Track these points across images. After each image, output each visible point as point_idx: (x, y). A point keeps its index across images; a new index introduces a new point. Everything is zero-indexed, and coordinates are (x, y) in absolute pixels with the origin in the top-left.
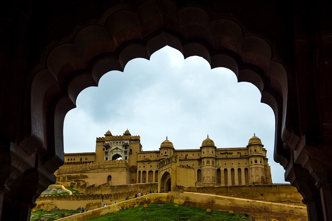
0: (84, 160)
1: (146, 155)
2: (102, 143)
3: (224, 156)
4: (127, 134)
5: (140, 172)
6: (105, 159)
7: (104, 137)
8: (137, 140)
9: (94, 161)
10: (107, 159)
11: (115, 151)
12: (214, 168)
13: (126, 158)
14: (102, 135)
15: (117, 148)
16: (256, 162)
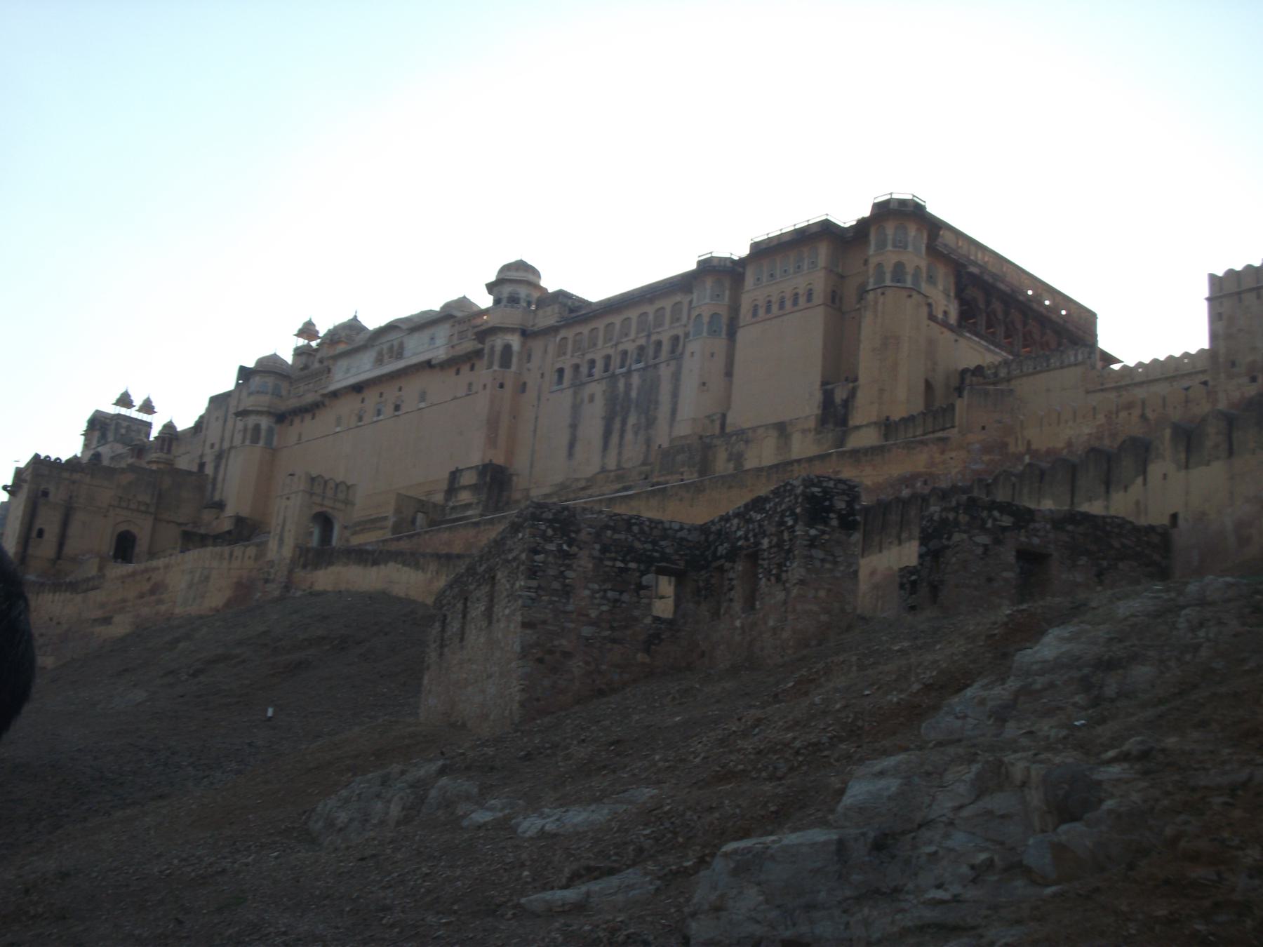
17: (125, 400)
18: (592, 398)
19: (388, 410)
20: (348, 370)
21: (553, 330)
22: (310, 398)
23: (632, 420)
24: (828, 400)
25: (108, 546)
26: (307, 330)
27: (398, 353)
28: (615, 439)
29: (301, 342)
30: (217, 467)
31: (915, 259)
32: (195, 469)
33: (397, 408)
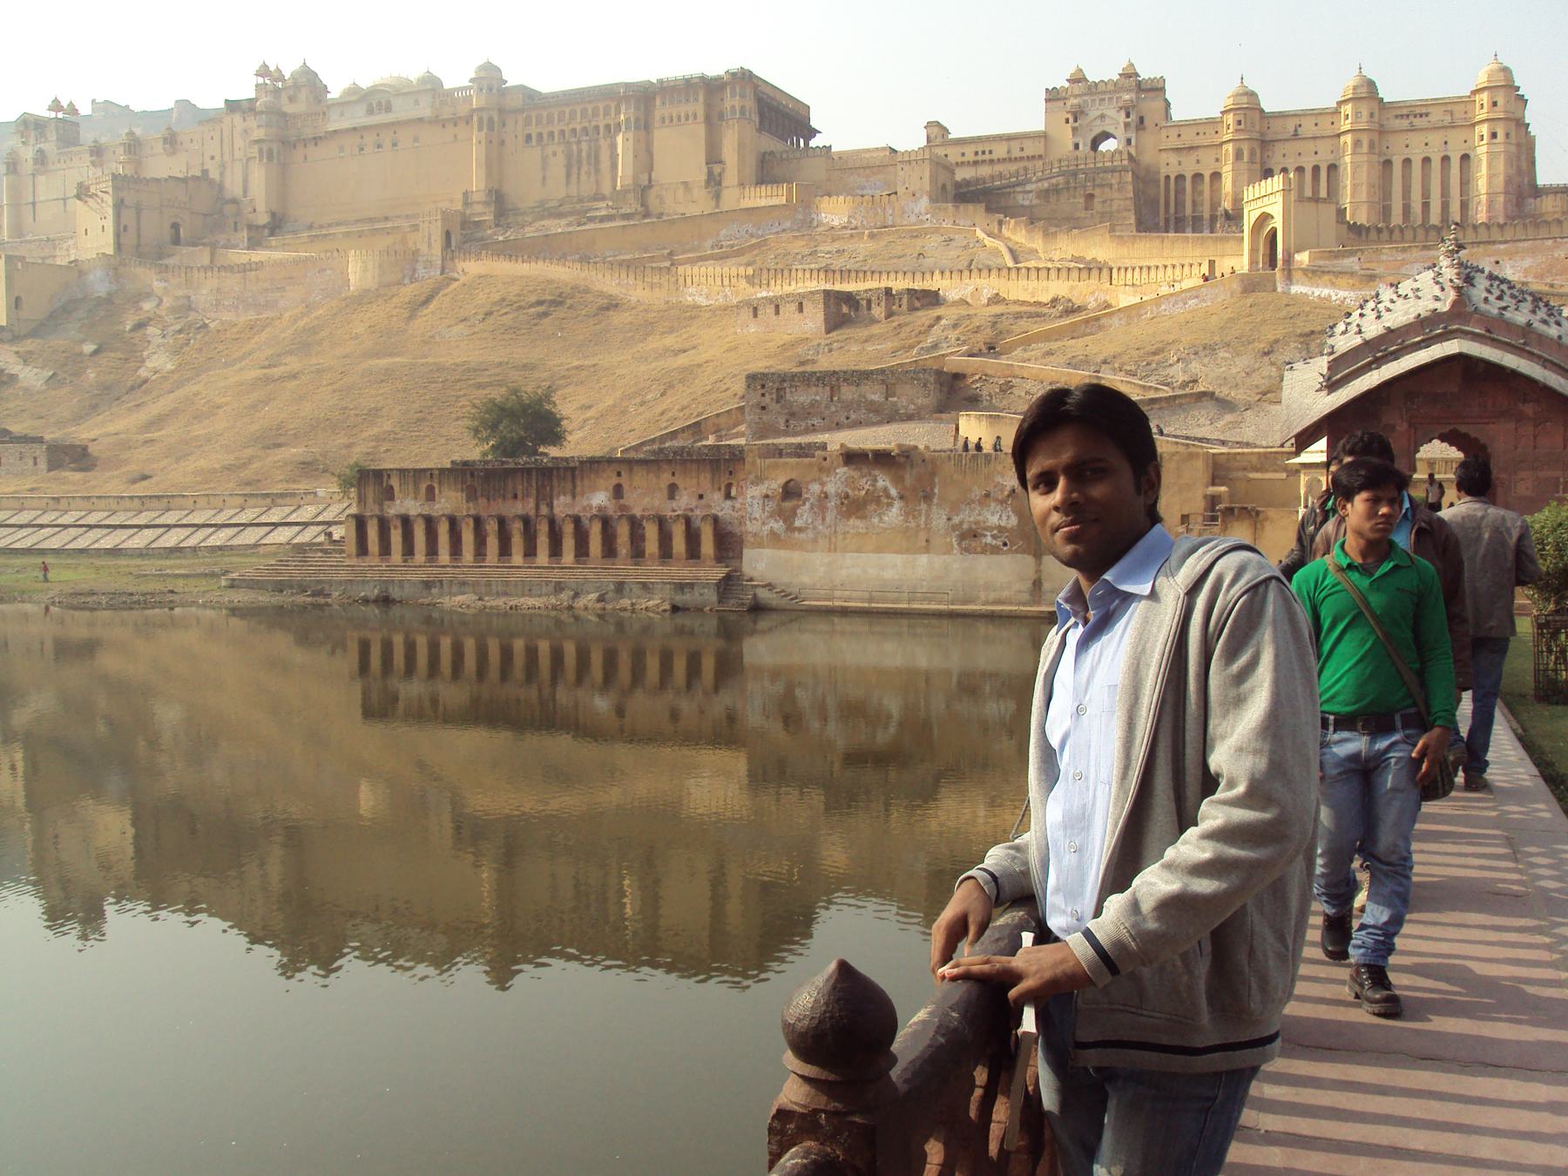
0: (1016, 153)
1: (1183, 131)
2: (1061, 103)
3: (1405, 123)
4: (1130, 74)
5: (1167, 177)
6: (1071, 147)
7: (1067, 85)
8: (1156, 89)
9: (1042, 152)
10: (1077, 146)
11: (1098, 122)
12: (1375, 158)
13: (1129, 142)
14: (1061, 82)
15: (1102, 117)
16: (1494, 135)
17: (56, 106)
18: (555, 154)
19: (387, 145)
20: (342, 114)
21: (521, 111)
22: (308, 132)
23: (585, 168)
24: (710, 173)
25: (167, 233)
26: (264, 71)
27: (389, 109)
28: (574, 177)
29: (261, 80)
30: (222, 174)
31: (750, 104)
32: (199, 174)
33: (395, 145)
